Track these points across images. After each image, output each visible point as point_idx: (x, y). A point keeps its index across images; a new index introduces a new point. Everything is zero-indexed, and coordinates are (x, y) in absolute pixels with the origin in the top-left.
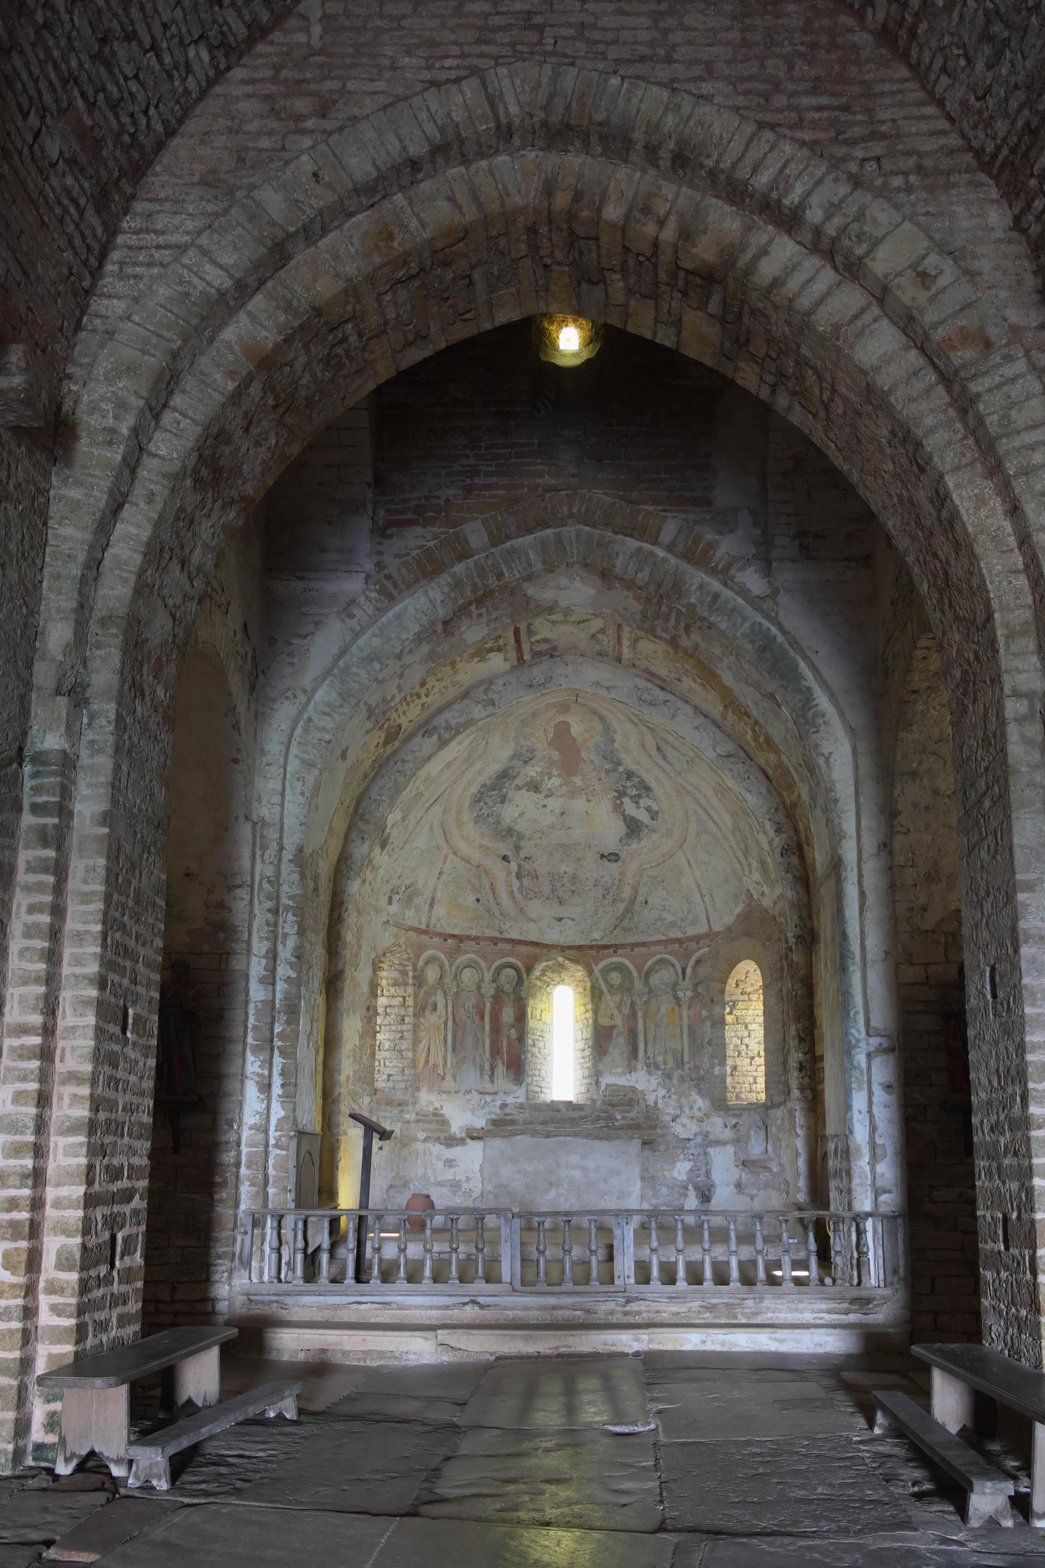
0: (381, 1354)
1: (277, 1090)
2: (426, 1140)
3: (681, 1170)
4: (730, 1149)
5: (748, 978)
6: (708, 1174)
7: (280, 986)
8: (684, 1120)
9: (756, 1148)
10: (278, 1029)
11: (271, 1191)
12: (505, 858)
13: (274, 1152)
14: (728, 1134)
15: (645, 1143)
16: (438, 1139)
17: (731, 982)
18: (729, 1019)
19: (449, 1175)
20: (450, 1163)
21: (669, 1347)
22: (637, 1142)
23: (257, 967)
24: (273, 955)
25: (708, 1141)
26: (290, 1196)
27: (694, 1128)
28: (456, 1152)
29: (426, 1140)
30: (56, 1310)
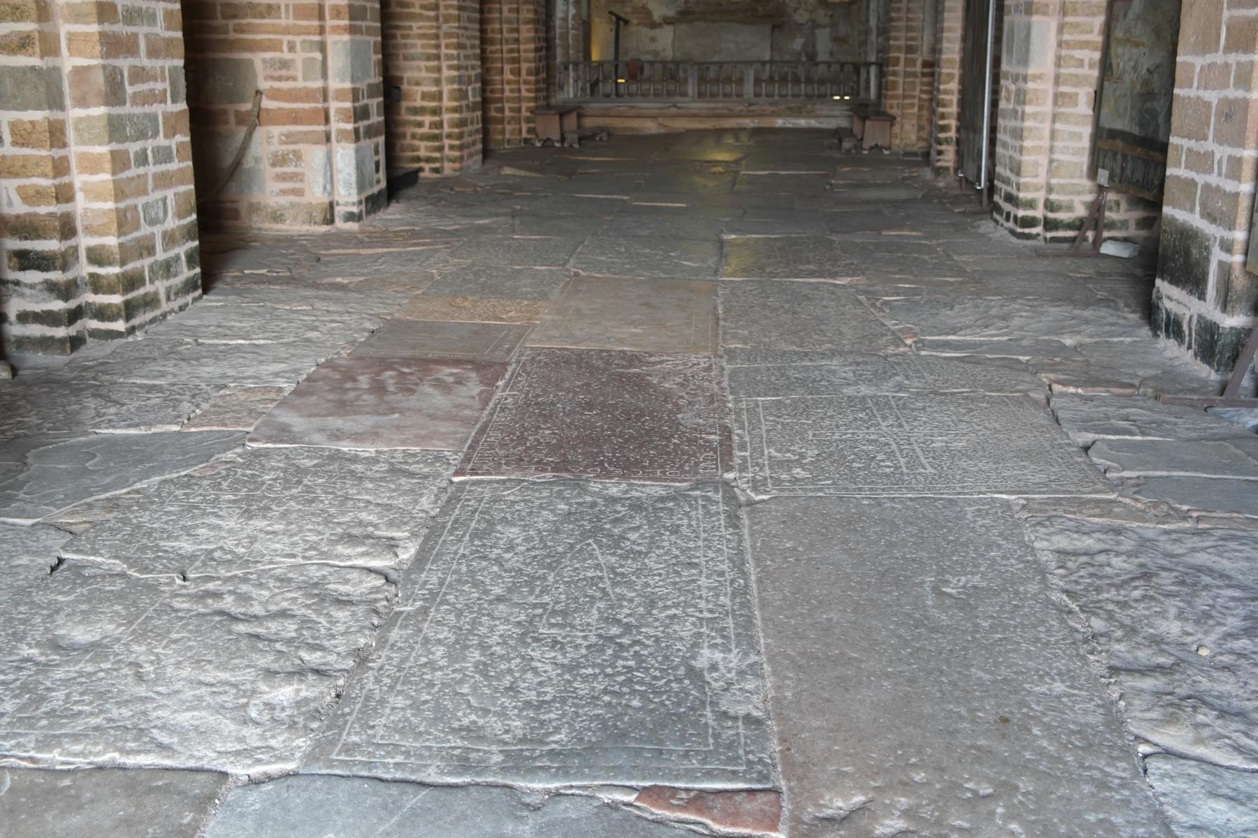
0: (632, 129)
2: (638, 24)
3: (798, 44)
4: (828, 30)
6: (814, 46)
8: (801, 11)
9: (843, 29)
11: (571, 52)
13: (572, 32)
14: (827, 21)
15: (774, 27)
16: (645, 24)
19: (652, 47)
20: (653, 39)
21: (768, 125)
22: (768, 28)
25: (815, 25)
26: (581, 55)
27: (807, 16)
28: (656, 32)
29: (638, 24)
30: (528, 90)
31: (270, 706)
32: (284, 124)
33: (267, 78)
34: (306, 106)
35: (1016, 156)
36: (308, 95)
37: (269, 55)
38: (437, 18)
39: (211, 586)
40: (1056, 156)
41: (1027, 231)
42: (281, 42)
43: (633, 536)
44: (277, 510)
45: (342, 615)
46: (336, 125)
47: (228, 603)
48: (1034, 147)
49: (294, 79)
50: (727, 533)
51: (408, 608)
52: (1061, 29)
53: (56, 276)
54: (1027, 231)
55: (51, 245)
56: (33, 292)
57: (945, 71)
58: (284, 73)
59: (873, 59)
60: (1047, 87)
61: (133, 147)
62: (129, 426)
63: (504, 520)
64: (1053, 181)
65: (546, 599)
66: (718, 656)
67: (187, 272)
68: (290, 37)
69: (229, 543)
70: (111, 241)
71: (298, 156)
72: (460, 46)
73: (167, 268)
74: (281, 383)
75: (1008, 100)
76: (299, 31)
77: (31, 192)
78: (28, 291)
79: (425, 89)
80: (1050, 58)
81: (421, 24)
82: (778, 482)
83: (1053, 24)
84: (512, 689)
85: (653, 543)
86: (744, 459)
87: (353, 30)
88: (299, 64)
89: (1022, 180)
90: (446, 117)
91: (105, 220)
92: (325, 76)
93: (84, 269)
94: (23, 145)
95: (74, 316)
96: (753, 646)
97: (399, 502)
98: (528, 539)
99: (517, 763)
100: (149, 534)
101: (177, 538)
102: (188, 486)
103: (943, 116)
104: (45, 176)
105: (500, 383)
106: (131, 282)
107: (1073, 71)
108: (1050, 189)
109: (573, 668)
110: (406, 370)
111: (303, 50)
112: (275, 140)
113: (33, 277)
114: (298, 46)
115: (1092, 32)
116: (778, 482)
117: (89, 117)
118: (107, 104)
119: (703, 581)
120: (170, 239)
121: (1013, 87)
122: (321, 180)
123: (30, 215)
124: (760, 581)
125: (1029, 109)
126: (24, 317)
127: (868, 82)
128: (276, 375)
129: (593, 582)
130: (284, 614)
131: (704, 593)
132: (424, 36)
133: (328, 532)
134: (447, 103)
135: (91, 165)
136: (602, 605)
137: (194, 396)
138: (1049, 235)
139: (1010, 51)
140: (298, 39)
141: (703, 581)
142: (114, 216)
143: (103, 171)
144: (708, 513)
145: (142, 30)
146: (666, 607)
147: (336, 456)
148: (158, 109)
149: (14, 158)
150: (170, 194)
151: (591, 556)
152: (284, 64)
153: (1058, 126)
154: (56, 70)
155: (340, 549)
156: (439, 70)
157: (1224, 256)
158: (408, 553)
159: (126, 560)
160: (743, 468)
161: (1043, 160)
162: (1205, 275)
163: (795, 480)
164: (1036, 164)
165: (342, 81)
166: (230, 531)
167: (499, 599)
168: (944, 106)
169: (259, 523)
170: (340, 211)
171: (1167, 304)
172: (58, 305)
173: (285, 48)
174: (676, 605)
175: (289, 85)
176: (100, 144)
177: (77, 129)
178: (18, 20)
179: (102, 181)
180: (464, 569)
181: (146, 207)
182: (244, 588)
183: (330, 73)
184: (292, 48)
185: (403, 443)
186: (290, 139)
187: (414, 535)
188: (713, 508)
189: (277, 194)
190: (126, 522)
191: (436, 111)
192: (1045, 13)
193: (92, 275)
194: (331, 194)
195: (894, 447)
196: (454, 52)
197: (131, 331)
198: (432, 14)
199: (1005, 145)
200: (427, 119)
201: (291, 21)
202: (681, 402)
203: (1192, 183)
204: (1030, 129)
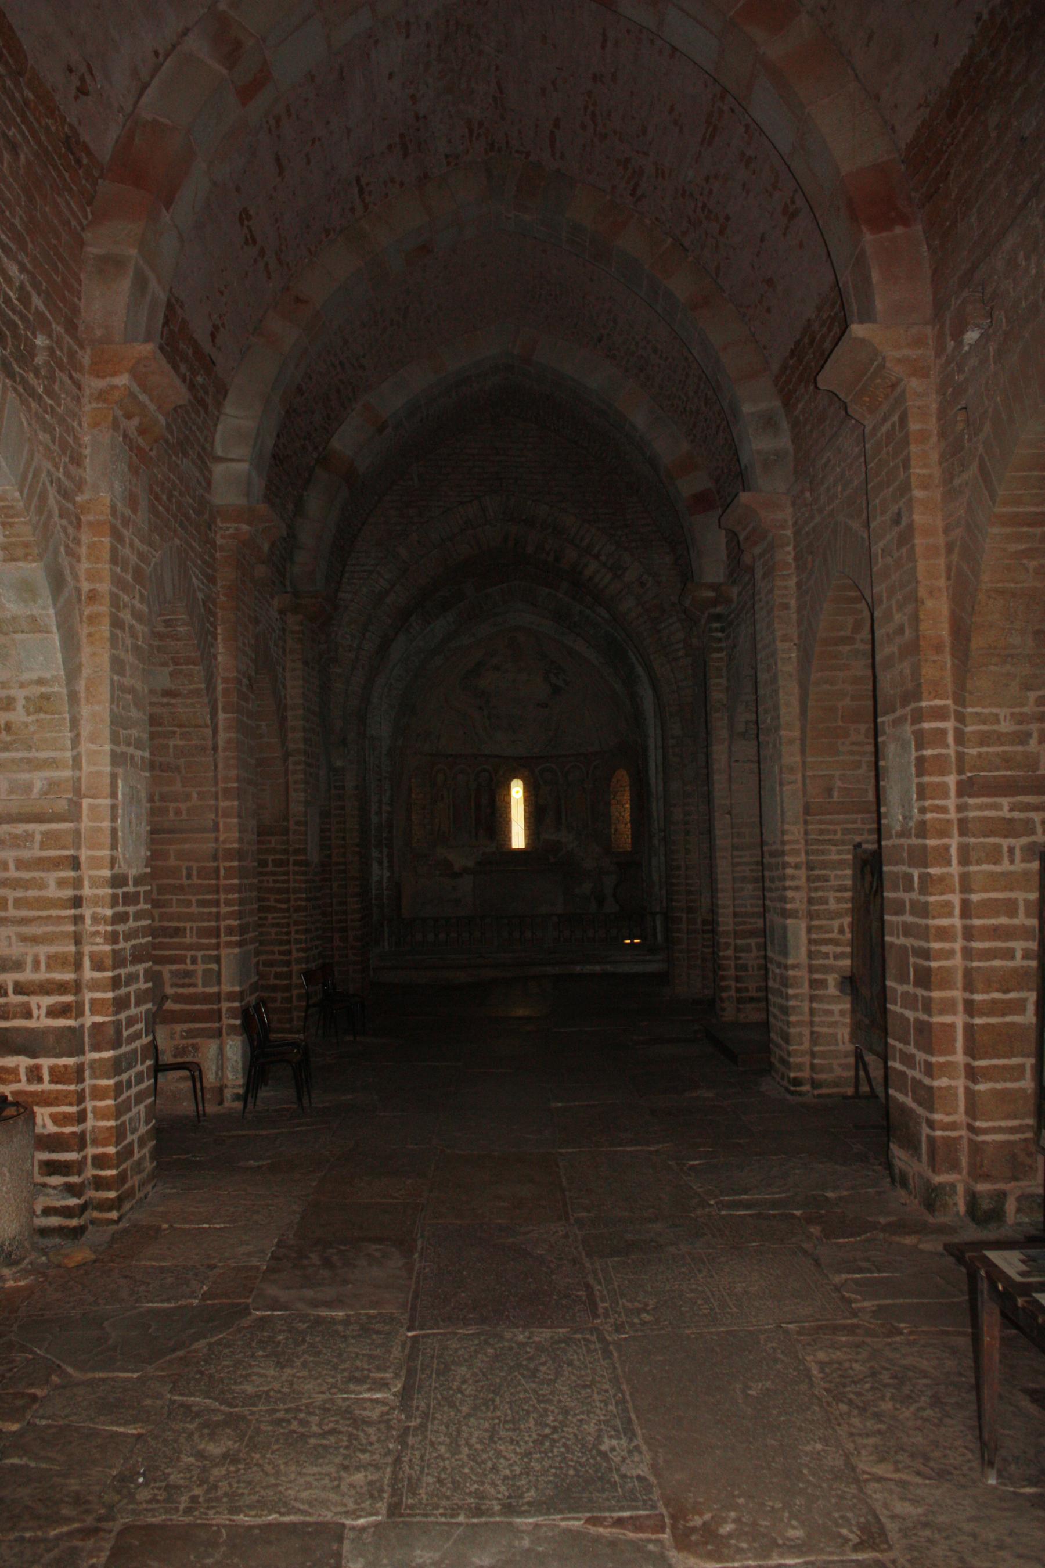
1: (386, 864)
5: (622, 777)
7: (384, 815)
10: (384, 835)
12: (480, 708)
17: (614, 780)
18: (613, 802)
23: (374, 807)
24: (380, 801)
31: (352, 1486)
32: (186, 1022)
33: (172, 986)
34: (205, 1007)
35: (785, 1028)
36: (206, 998)
37: (175, 967)
38: (288, 910)
39: (278, 1415)
40: (816, 1029)
41: (798, 1089)
42: (186, 956)
43: (543, 1369)
44: (298, 1363)
45: (371, 1430)
46: (226, 1021)
47: (295, 1425)
48: (798, 1021)
49: (195, 985)
50: (605, 1363)
51: (413, 1424)
52: (810, 930)
53: (74, 1179)
54: (798, 1089)
55: (72, 1156)
56: (56, 1192)
57: (722, 940)
58: (187, 981)
59: (658, 910)
60: (802, 973)
61: (125, 1077)
62: (162, 1301)
63: (453, 1362)
64: (816, 1049)
65: (499, 1413)
66: (614, 1442)
67: (149, 1166)
68: (193, 953)
69: (276, 1386)
70: (111, 1150)
71: (196, 1047)
72: (307, 931)
73: (138, 1167)
74: (255, 1262)
75: (774, 980)
76: (200, 947)
77: (61, 1117)
78: (52, 1192)
79: (279, 969)
80: (803, 951)
81: (276, 915)
82: (632, 1325)
83: (803, 925)
84: (494, 1469)
85: (558, 1373)
86: (606, 1309)
87: (240, 944)
88: (200, 973)
89: (791, 1048)
90: (295, 992)
91: (107, 1135)
92: (219, 983)
93: (90, 1172)
94: (57, 1083)
95: (83, 1208)
96: (634, 1435)
97: (378, 1352)
98: (475, 1374)
99: (509, 1509)
100: (221, 1380)
101: (241, 1383)
102: (230, 1346)
103: (723, 978)
104: (71, 1104)
105: (416, 1256)
106: (122, 1178)
107: (821, 962)
108: (813, 1055)
109: (528, 1454)
110: (343, 1248)
111: (203, 962)
112: (177, 1036)
113: (56, 1180)
114: (199, 959)
115: (833, 932)
116: (632, 1325)
117: (101, 1059)
118: (113, 1049)
119: (596, 1396)
120: (142, 1142)
121: (777, 971)
122: (214, 1068)
123: (57, 1134)
124: (631, 1394)
125: (791, 991)
126: (47, 1211)
127: (654, 928)
128: (249, 1255)
129: (527, 1400)
130: (333, 1432)
131: (598, 1404)
132: (277, 925)
133: (339, 1376)
134: (295, 980)
135: (98, 1093)
136: (535, 1415)
137: (196, 1275)
138: (815, 1092)
139: (772, 943)
140: (200, 954)
141: (596, 1396)
142: (114, 1131)
143: (109, 1098)
144: (589, 1351)
145: (132, 989)
146: (575, 1415)
147: (319, 1321)
148: (137, 1044)
149: (50, 1092)
150: (142, 1107)
151: (520, 1384)
152: (188, 974)
153: (814, 1005)
154: (82, 1026)
155: (352, 1387)
156: (289, 952)
157: (928, 1131)
158: (398, 1386)
159: (216, 1399)
160: (606, 1316)
161: (806, 1032)
162: (920, 1142)
163: (644, 1323)
164: (800, 1034)
165: (233, 986)
166: (272, 1377)
167: (468, 1416)
168: (724, 970)
169: (289, 1371)
170: (228, 1094)
171: (897, 1163)
172: (73, 1202)
173: (188, 961)
174: (583, 1413)
175: (192, 990)
176: (109, 1078)
177: (91, 1067)
178: (62, 994)
179: (107, 1106)
180: (439, 1396)
181: (131, 1120)
182: (302, 1415)
183: (223, 980)
184: (194, 961)
185: (363, 1308)
186: (191, 1034)
187: (397, 1376)
188: (592, 1347)
189: (177, 1081)
190: (202, 1373)
191: (287, 988)
192: (796, 917)
193: (95, 1177)
194: (221, 1079)
195: (709, 1293)
196: (303, 937)
197: (120, 1218)
198: (284, 906)
199: (775, 1016)
200: (279, 995)
201: (195, 940)
202: (552, 1266)
203: (904, 1074)
204: (793, 1007)
